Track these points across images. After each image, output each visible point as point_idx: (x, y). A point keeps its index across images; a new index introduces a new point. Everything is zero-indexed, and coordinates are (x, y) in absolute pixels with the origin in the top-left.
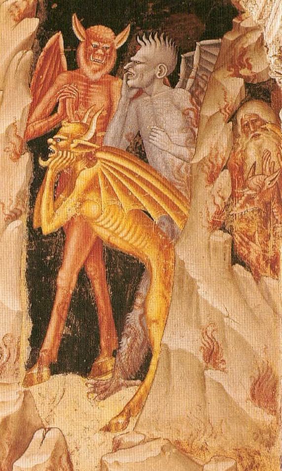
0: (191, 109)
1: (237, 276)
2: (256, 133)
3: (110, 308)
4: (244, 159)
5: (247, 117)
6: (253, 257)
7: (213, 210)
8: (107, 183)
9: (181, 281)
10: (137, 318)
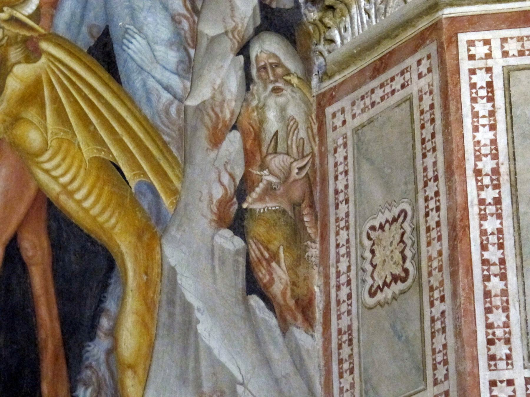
0: (184, 16)
1: (254, 313)
2: (277, 84)
3: (57, 325)
4: (262, 121)
5: (264, 56)
6: (277, 289)
7: (218, 193)
8: (56, 99)
9: (171, 302)
10: (103, 357)
